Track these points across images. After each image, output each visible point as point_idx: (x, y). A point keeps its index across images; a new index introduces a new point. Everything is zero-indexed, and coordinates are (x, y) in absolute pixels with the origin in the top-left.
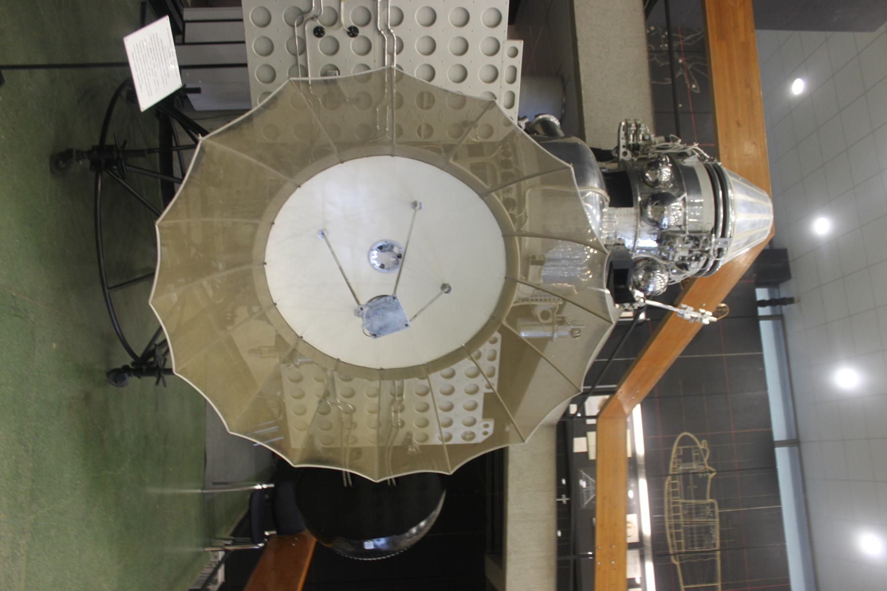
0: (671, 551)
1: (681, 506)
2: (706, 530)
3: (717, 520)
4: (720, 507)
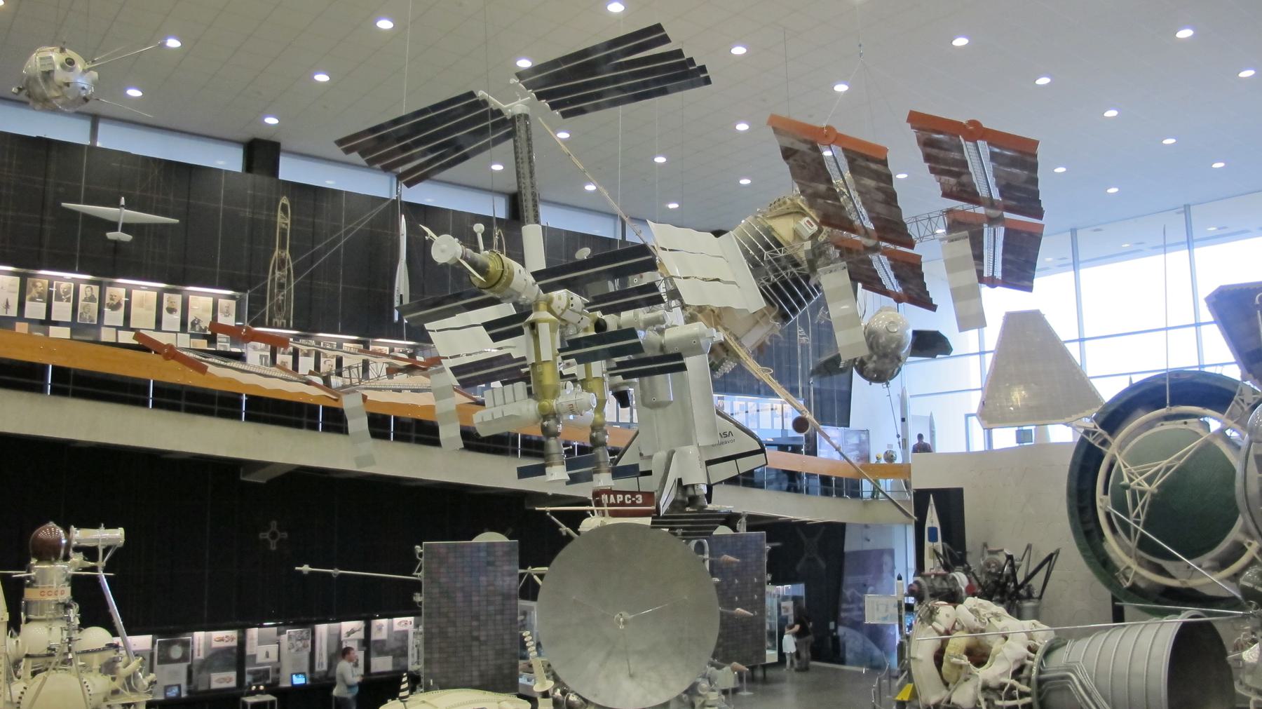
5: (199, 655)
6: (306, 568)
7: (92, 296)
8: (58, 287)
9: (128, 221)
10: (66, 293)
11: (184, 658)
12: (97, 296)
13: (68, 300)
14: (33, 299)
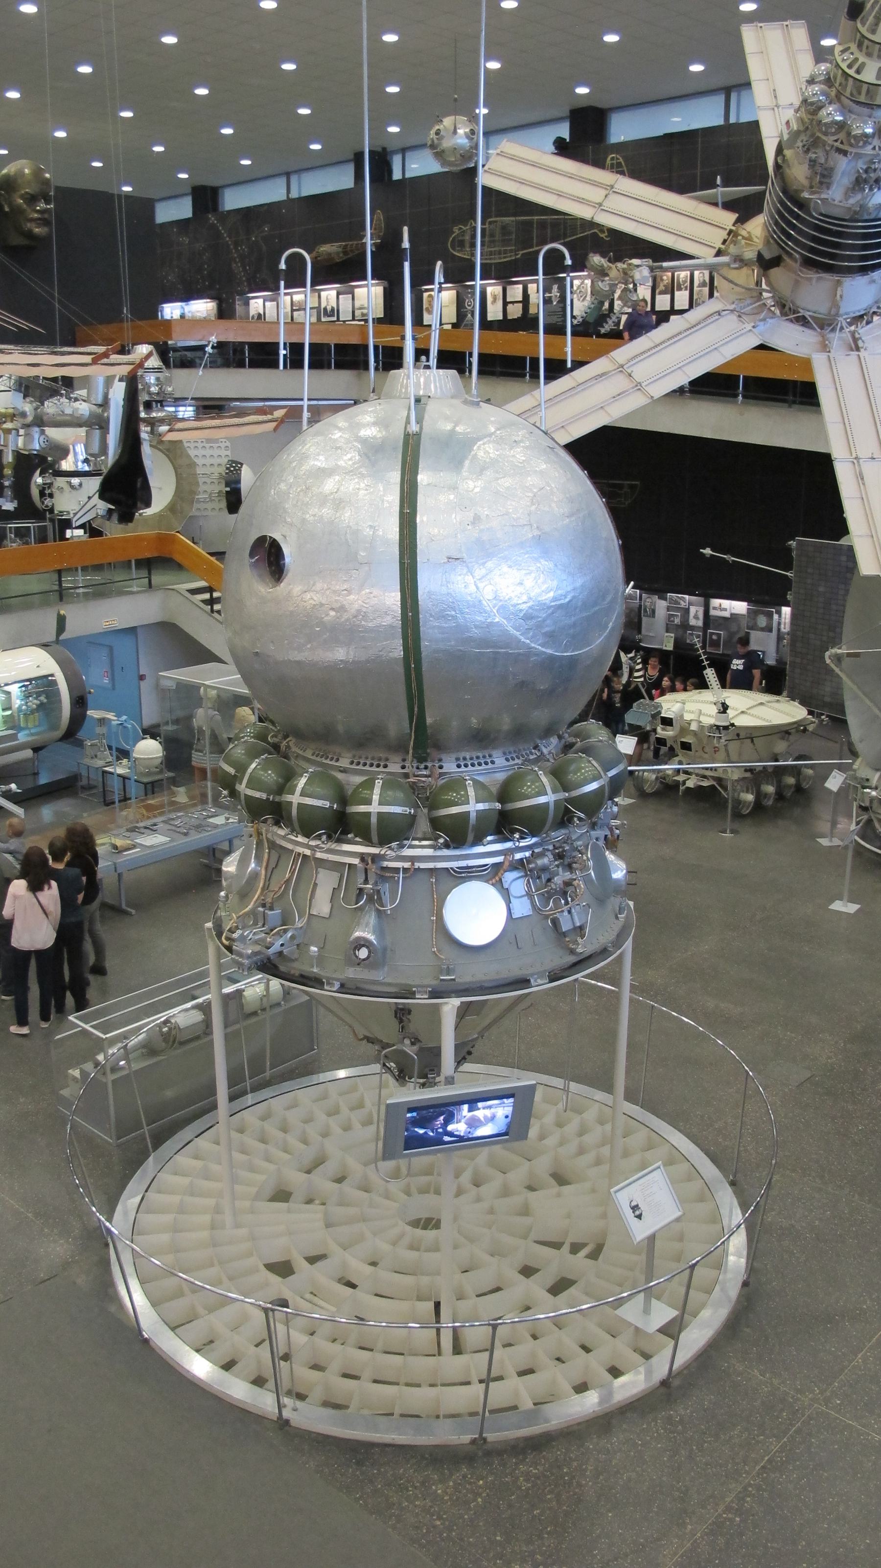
0: (513, 258)
1: (490, 249)
2: (504, 228)
3: (498, 219)
4: (491, 217)
5: (785, 628)
6: (708, 551)
7: (704, 281)
8: (678, 276)
9: (726, 199)
10: (685, 282)
11: (769, 629)
12: (707, 280)
13: (686, 289)
14: (661, 293)
